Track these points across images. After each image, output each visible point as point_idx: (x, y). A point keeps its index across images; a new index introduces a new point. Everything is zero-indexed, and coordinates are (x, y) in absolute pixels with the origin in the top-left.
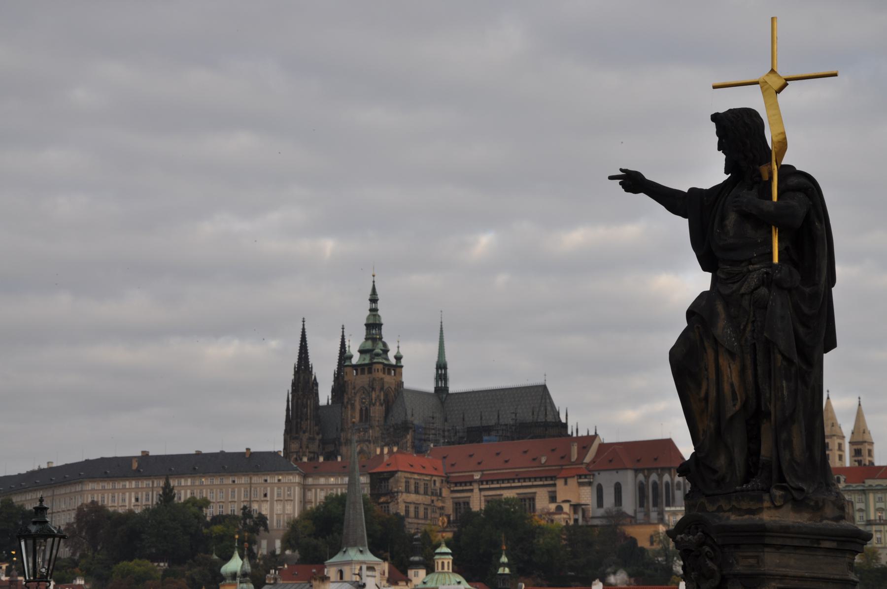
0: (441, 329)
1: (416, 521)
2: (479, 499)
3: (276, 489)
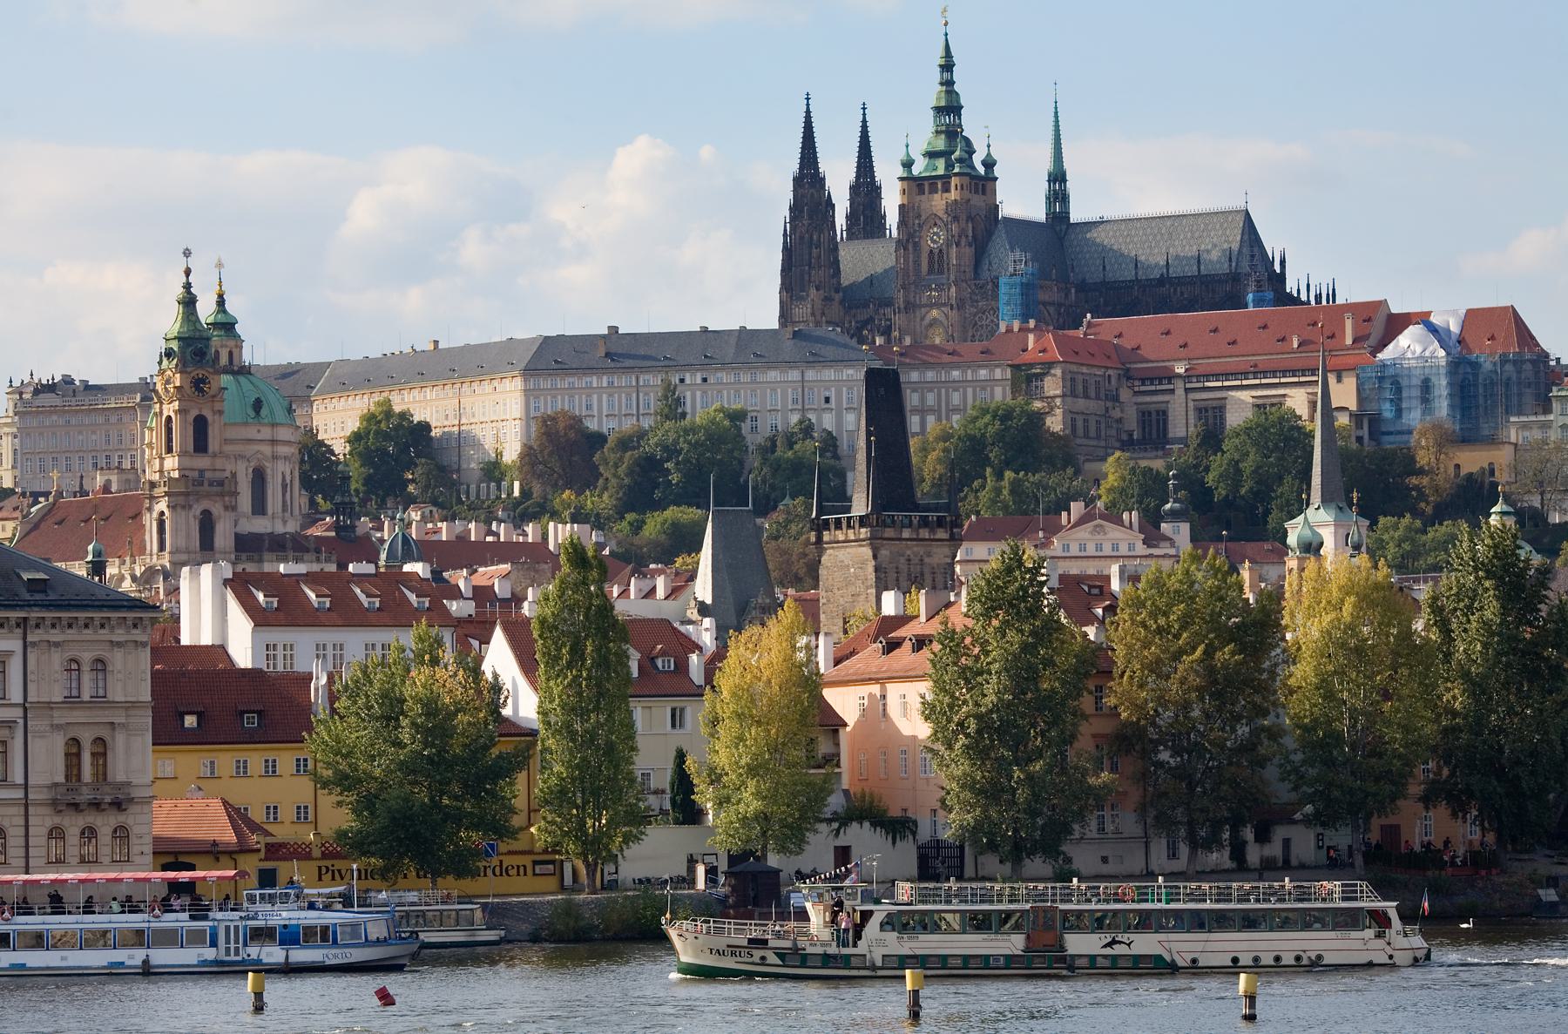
0: (1056, 113)
1: (1086, 442)
2: (1184, 405)
3: (844, 389)
